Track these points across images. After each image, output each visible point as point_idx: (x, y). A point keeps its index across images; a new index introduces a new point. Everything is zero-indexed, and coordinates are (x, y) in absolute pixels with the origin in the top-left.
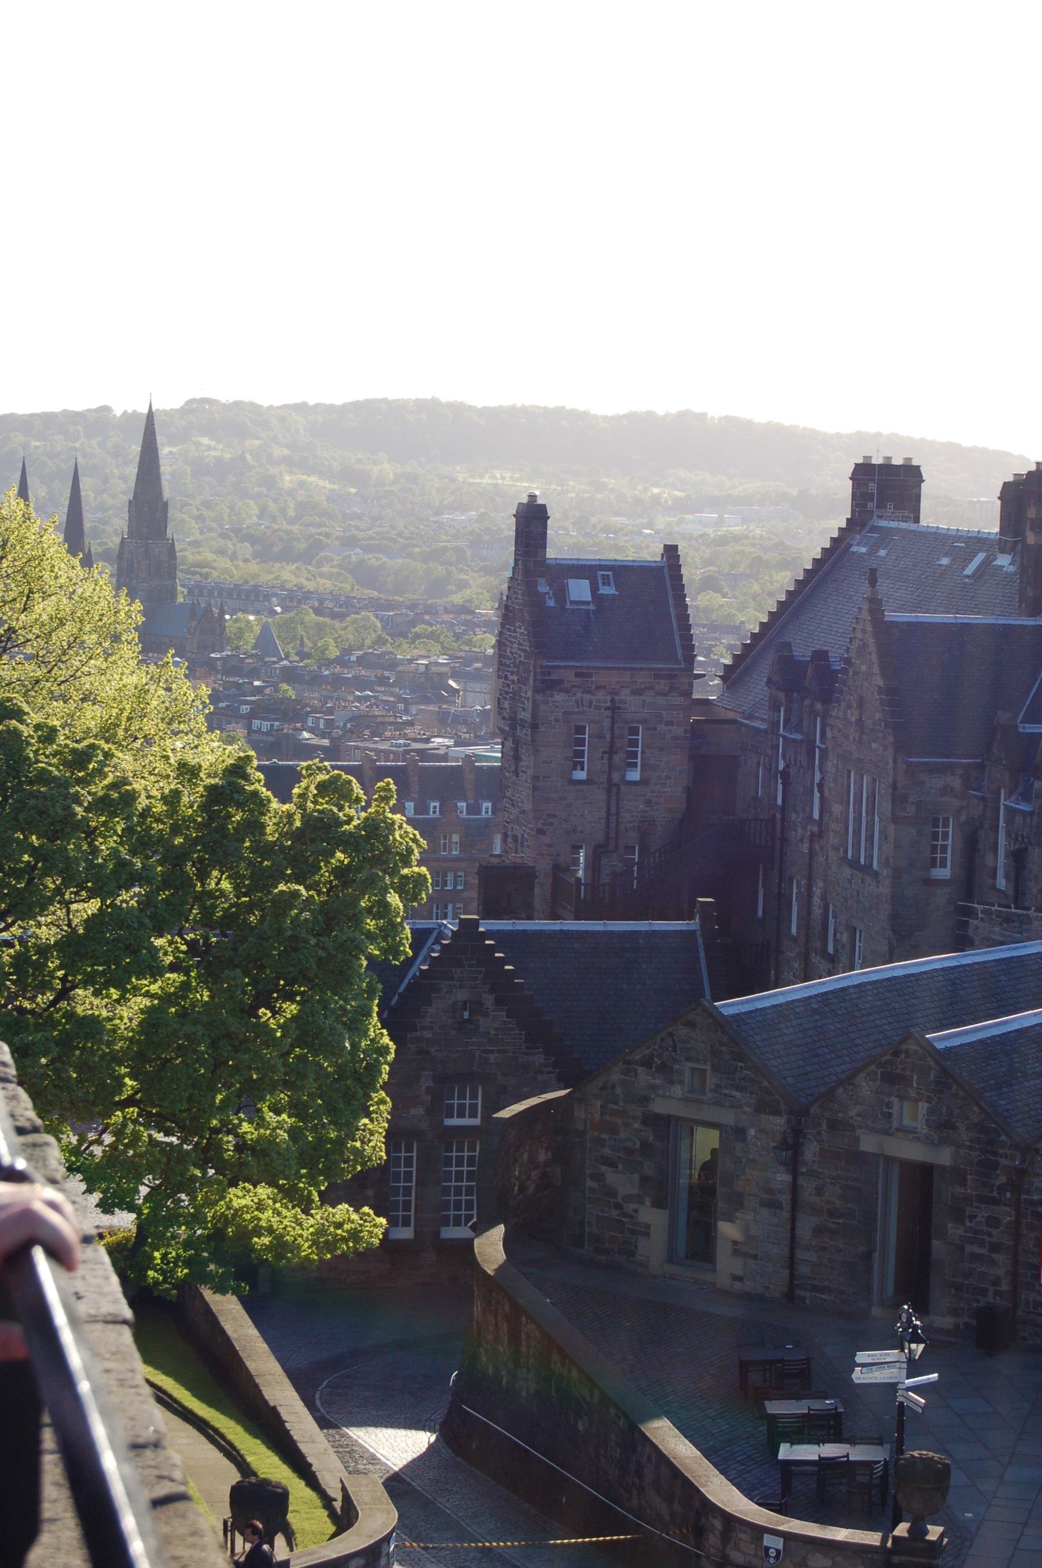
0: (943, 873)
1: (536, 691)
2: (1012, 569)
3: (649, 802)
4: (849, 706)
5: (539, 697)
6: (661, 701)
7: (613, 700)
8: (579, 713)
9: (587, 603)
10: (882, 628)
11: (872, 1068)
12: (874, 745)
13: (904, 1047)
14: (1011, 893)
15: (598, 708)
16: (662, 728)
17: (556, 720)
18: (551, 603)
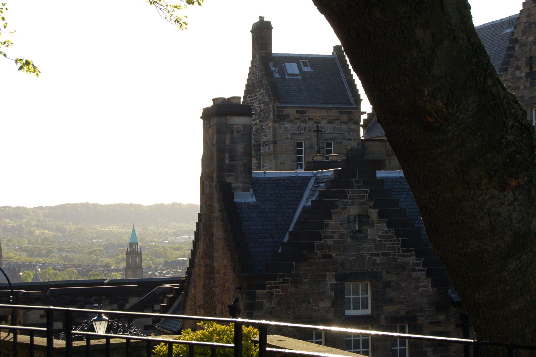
1: (275, 121)
5: (276, 125)
6: (344, 127)
7: (317, 127)
8: (299, 134)
9: (297, 75)
16: (345, 142)
17: (287, 138)
18: (277, 75)
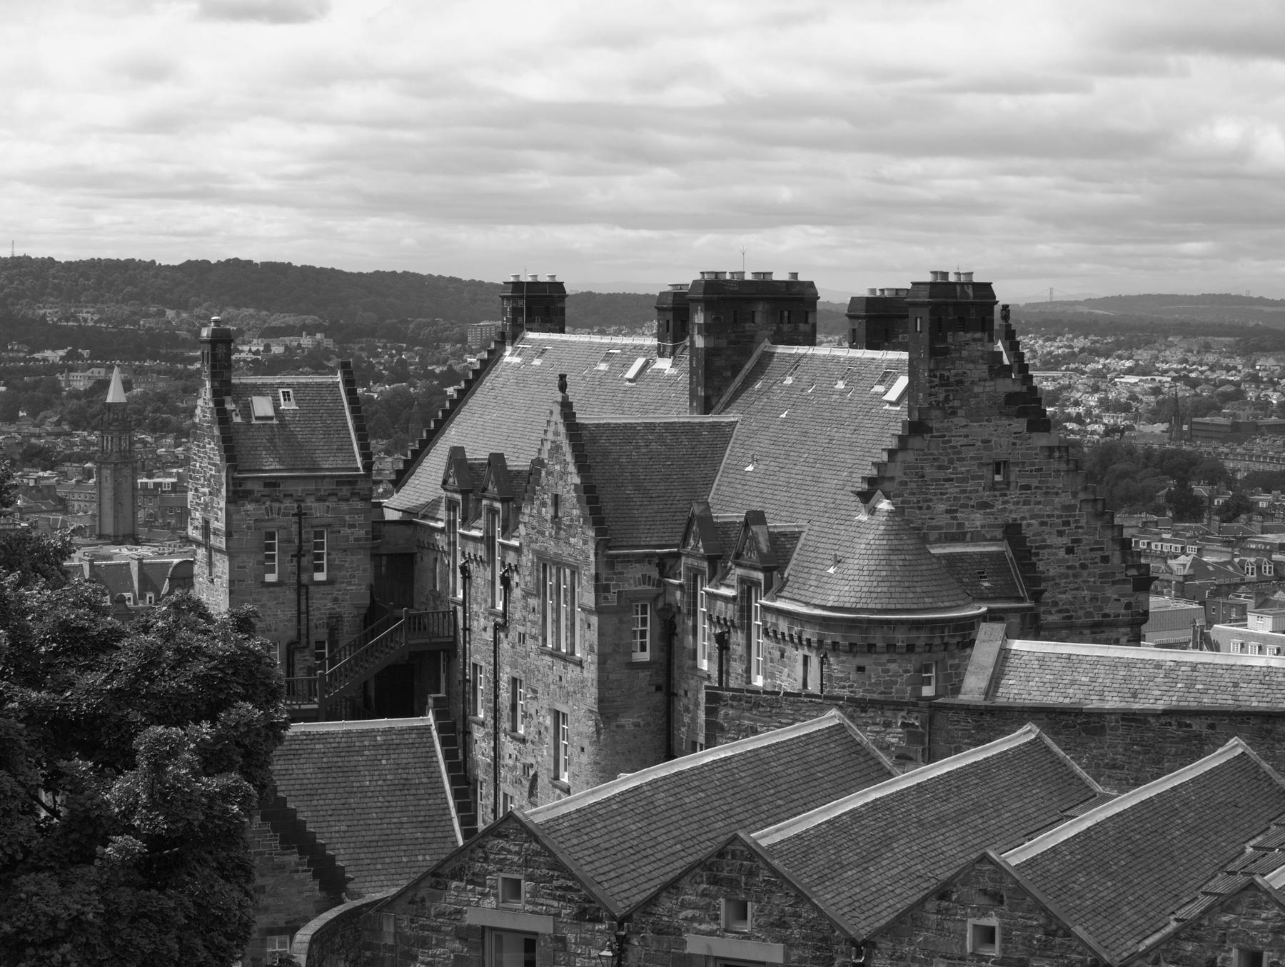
0: (645, 656)
2: (674, 371)
3: (335, 600)
4: (544, 504)
5: (232, 507)
6: (344, 506)
7: (299, 507)
8: (268, 520)
9: (271, 418)
10: (574, 429)
11: (698, 870)
12: (572, 540)
13: (730, 847)
14: (715, 674)
15: (285, 515)
17: (249, 528)
18: (238, 420)
